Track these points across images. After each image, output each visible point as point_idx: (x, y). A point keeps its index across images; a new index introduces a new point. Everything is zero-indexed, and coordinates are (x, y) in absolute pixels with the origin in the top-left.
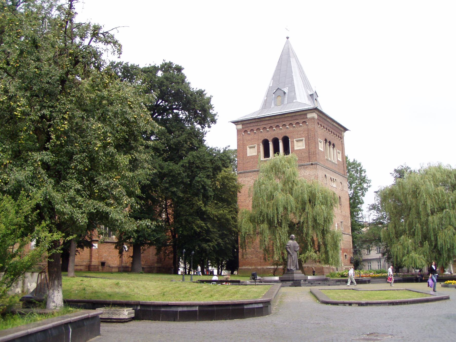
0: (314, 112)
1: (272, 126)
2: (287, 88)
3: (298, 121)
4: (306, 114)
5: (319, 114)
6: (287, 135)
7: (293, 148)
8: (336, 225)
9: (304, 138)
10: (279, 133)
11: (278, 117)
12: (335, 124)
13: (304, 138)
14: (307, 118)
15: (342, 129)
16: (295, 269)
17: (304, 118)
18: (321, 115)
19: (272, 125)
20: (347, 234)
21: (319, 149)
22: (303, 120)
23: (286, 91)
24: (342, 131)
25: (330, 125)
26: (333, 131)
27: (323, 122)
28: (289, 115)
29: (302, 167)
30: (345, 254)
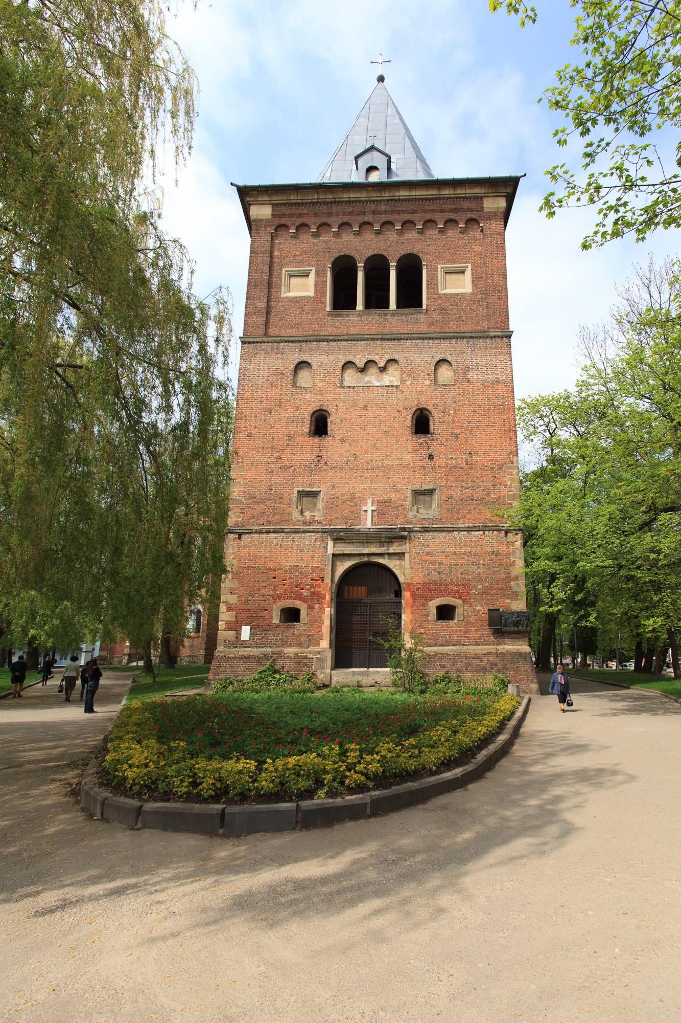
8: (369, 507)
12: (403, 193)
15: (477, 191)
20: (469, 530)
24: (480, 199)
25: (372, 207)
30: (433, 604)
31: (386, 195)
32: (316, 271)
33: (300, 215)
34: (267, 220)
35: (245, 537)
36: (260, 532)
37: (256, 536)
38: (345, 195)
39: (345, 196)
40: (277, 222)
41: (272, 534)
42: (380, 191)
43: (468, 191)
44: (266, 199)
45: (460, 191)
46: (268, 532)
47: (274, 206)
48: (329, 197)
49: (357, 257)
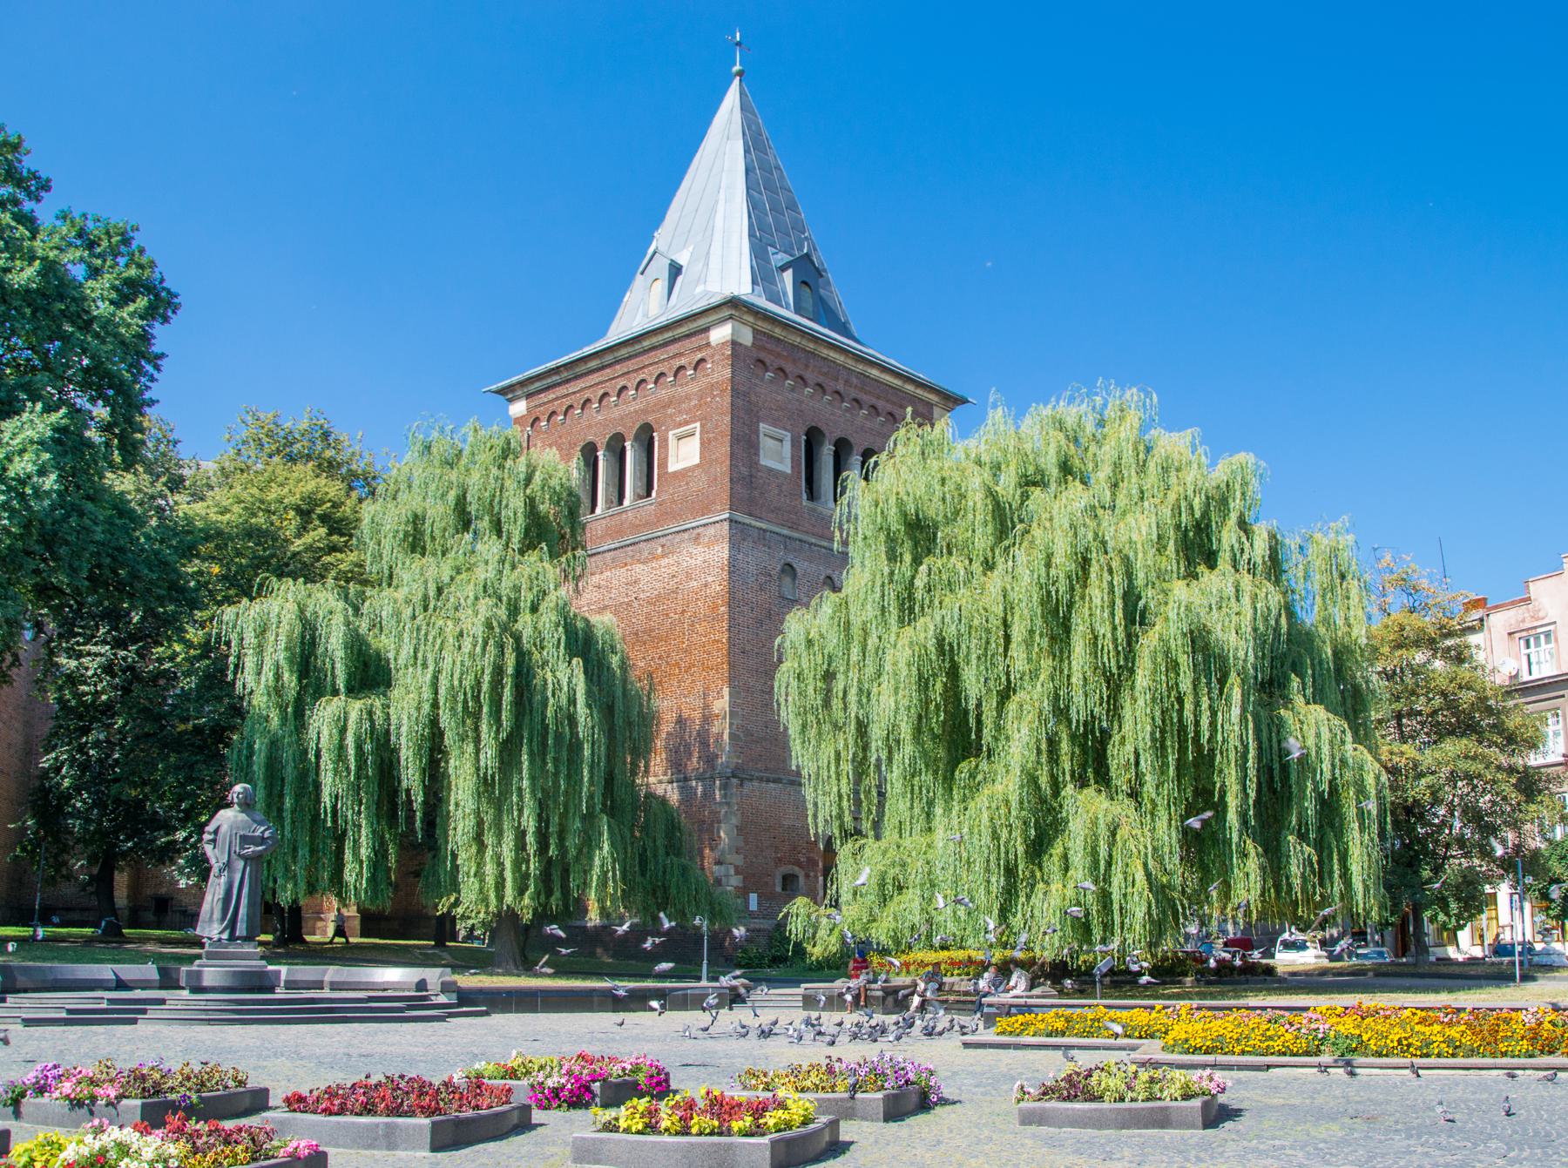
0: (731, 317)
1: (607, 390)
2: (691, 249)
3: (683, 361)
4: (706, 330)
5: (764, 326)
6: (650, 419)
7: (664, 464)
9: (698, 425)
10: (621, 414)
11: (624, 352)
12: (875, 372)
13: (698, 425)
14: (708, 344)
15: (933, 398)
16: (225, 936)
17: (699, 348)
18: (778, 332)
19: (608, 387)
21: (757, 463)
22: (699, 356)
23: (682, 260)
26: (867, 399)
27: (794, 361)
28: (655, 340)
29: (686, 535)
31: (860, 367)
32: (792, 441)
33: (779, 355)
34: (746, 347)
35: (747, 785)
36: (761, 779)
37: (756, 784)
38: (825, 351)
39: (825, 352)
40: (755, 354)
41: (772, 785)
42: (857, 361)
43: (926, 394)
44: (751, 319)
45: (919, 391)
46: (768, 781)
47: (756, 332)
48: (811, 345)
49: (827, 434)
